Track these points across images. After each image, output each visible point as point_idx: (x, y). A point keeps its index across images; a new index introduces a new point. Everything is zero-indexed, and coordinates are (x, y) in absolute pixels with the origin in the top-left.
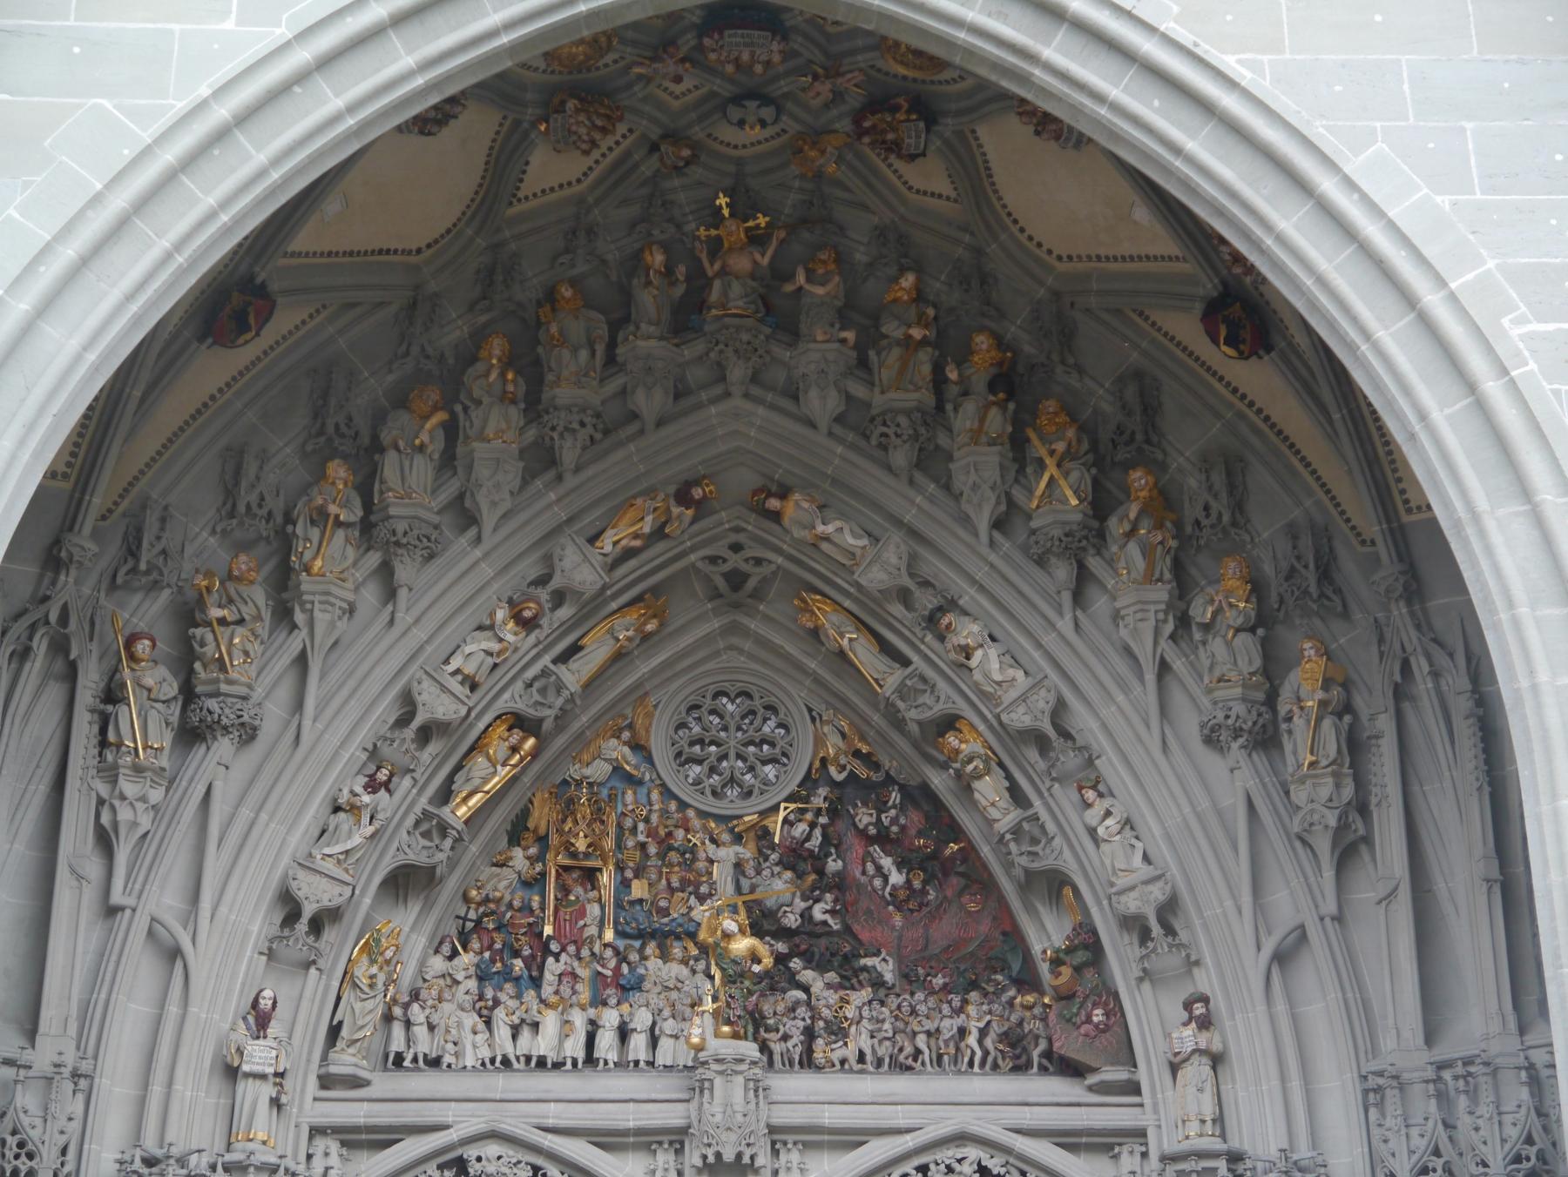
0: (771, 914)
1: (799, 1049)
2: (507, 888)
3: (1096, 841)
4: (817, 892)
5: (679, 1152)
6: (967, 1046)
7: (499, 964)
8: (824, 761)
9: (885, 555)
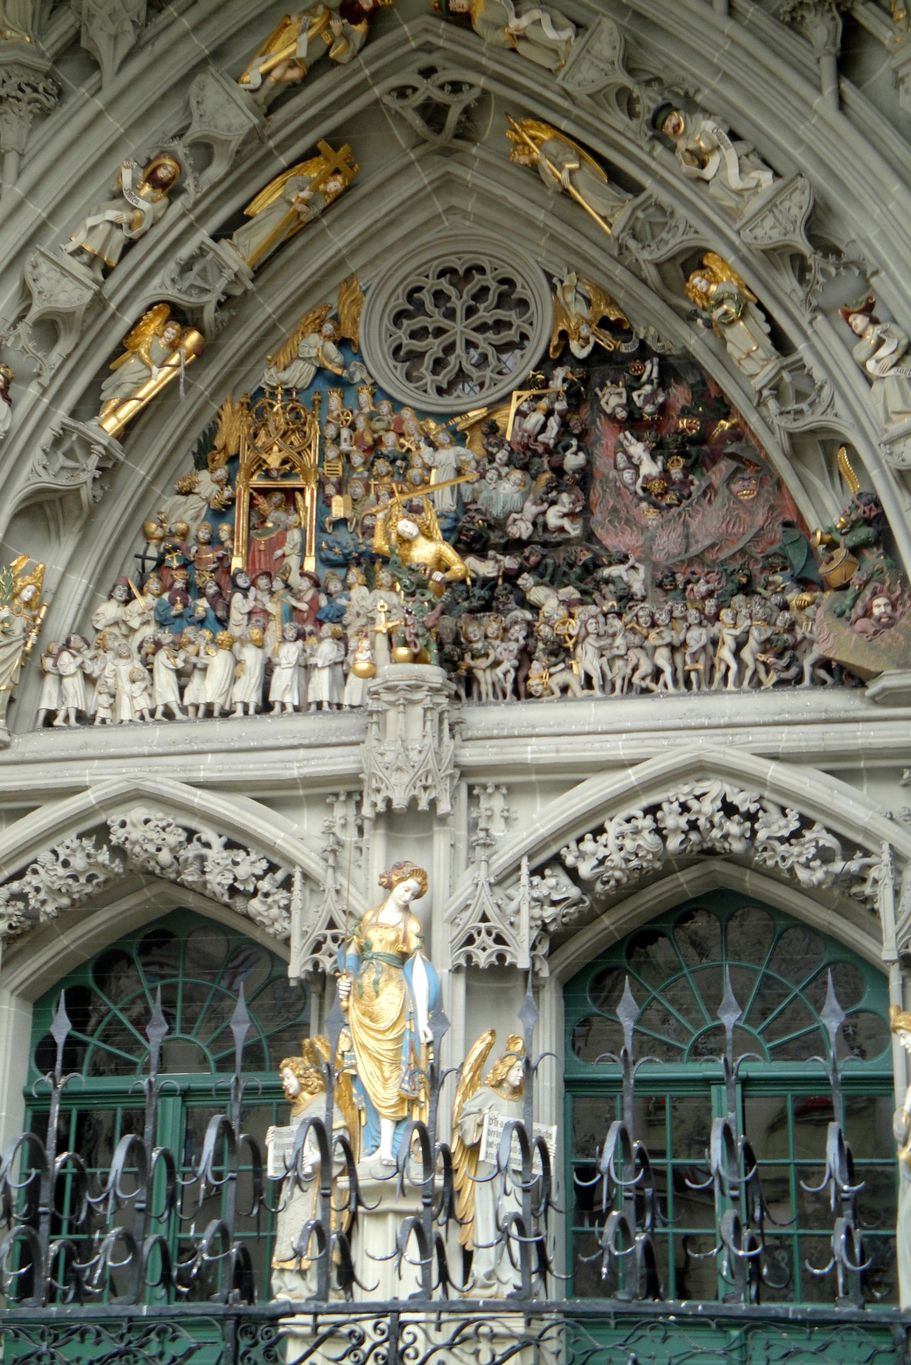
0: (498, 525)
1: (511, 676)
2: (195, 518)
3: (869, 381)
4: (554, 493)
5: (359, 805)
6: (721, 660)
7: (179, 606)
8: (564, 335)
9: (597, 47)
